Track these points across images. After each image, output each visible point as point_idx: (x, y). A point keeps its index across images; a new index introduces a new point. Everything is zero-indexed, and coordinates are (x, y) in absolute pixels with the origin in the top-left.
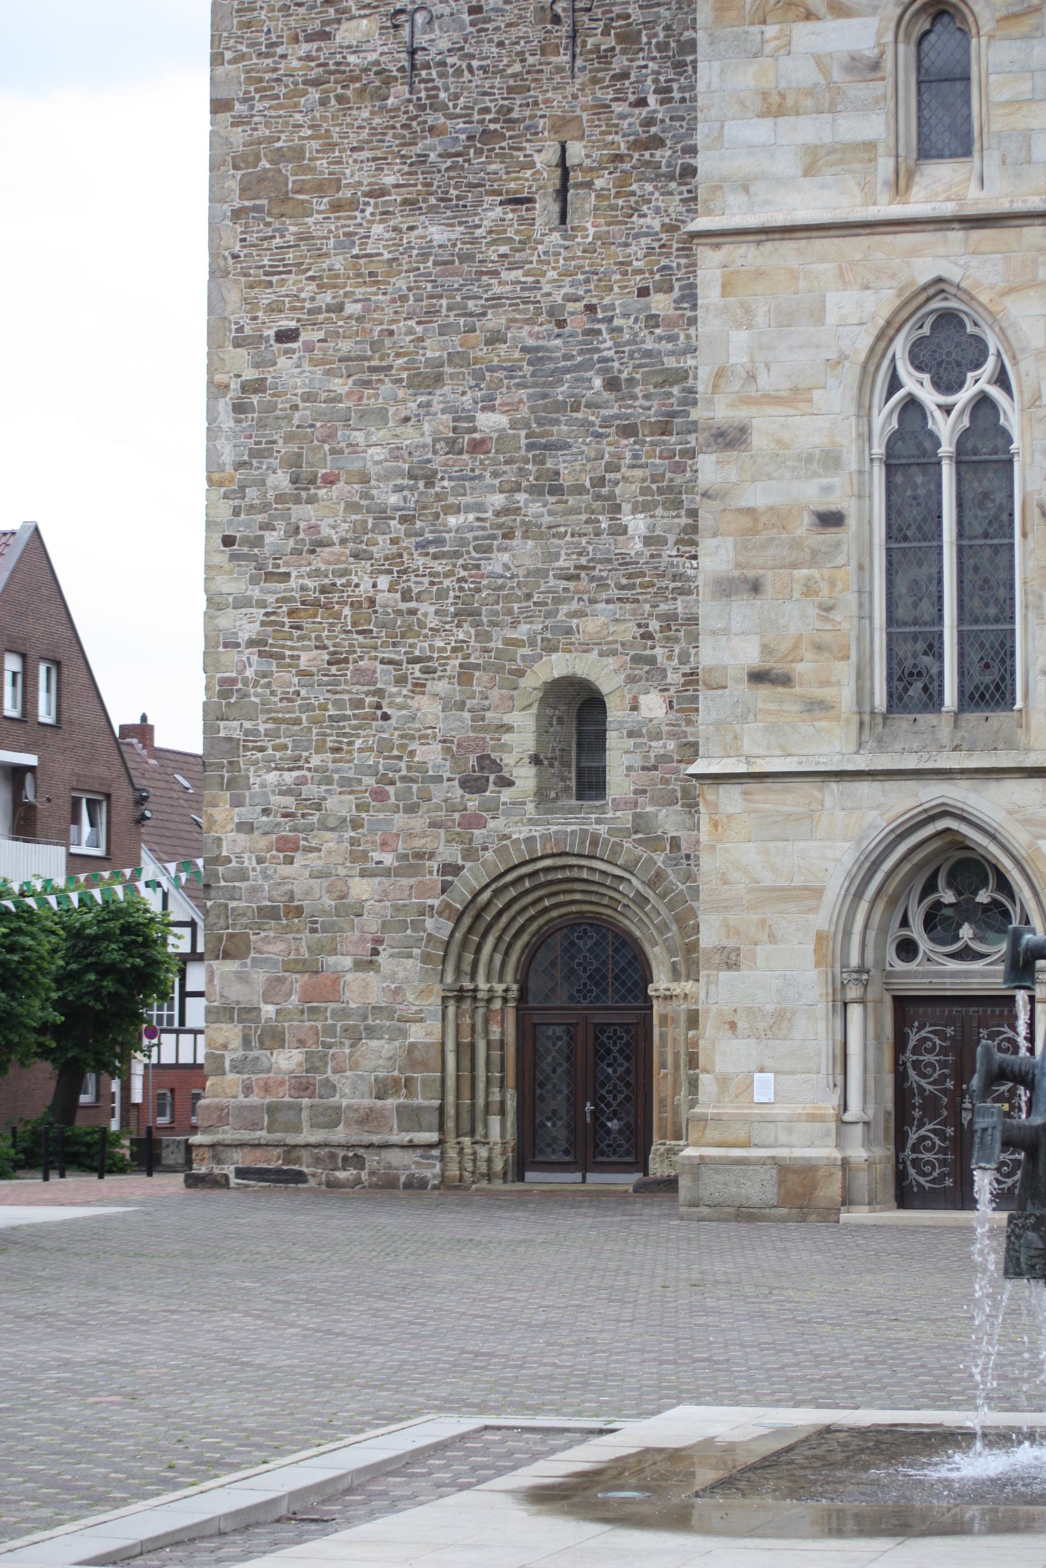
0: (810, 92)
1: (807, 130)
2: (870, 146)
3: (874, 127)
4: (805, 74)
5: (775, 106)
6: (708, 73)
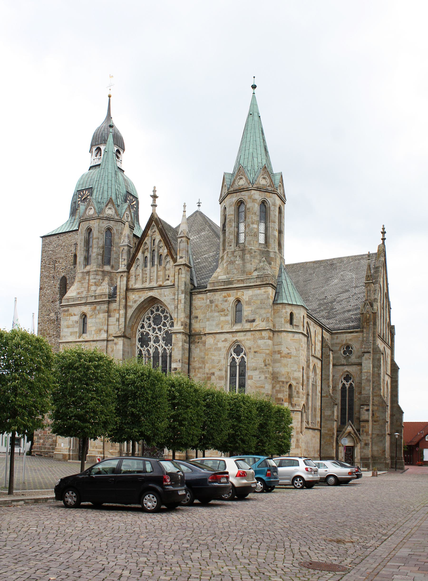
0: (71, 325)
1: (71, 330)
2: (77, 332)
3: (77, 330)
4: (71, 323)
5: (68, 327)
6: (62, 323)
